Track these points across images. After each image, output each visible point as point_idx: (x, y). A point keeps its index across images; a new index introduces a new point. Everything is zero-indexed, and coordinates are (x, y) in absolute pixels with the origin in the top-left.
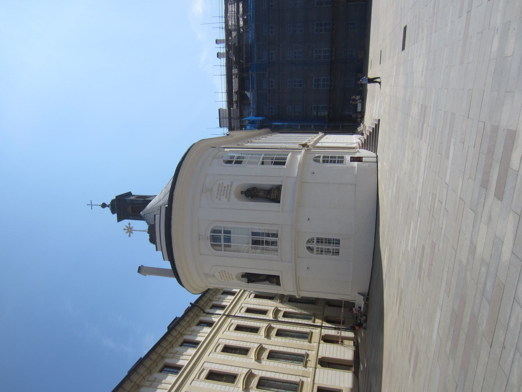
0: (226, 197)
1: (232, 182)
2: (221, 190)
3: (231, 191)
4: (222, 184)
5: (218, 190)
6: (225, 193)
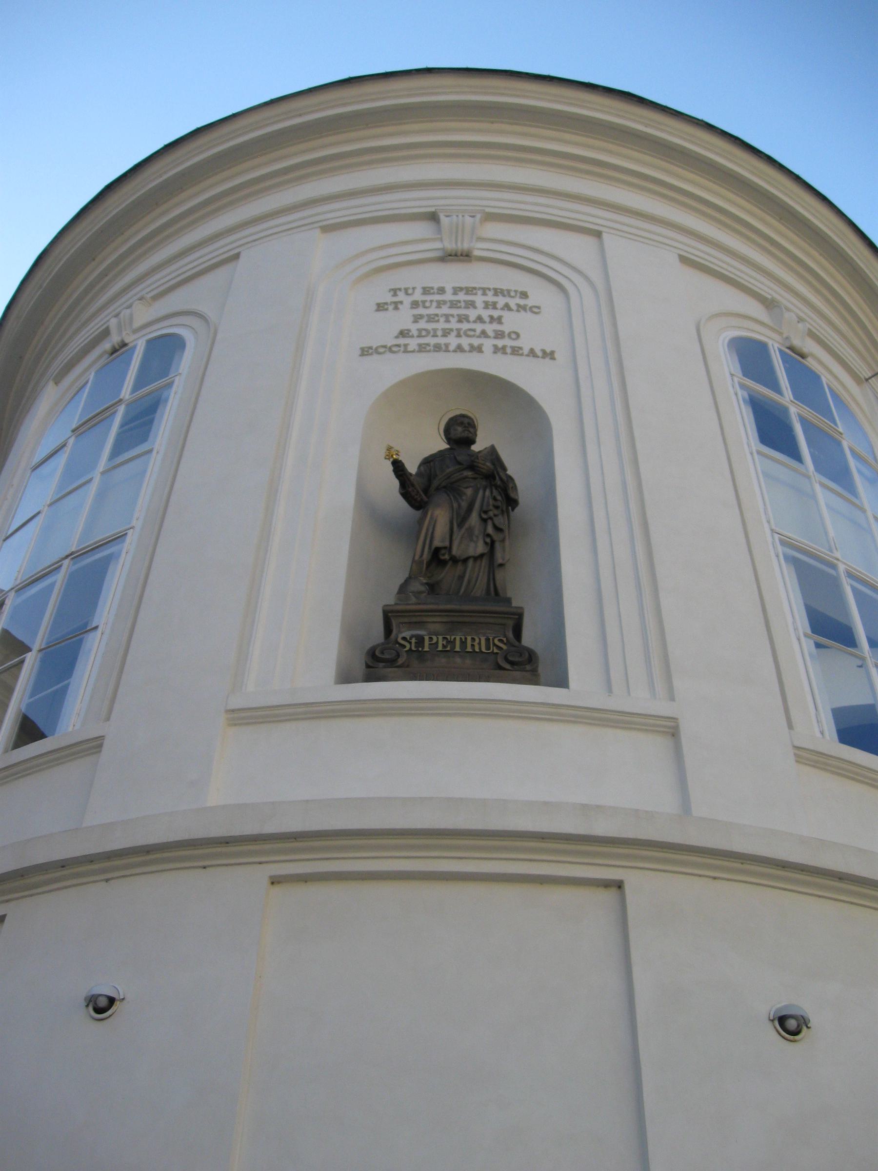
0: (403, 334)
1: (550, 355)
2: (471, 305)
3: (459, 349)
4: (518, 306)
5: (470, 291)
6: (430, 326)
